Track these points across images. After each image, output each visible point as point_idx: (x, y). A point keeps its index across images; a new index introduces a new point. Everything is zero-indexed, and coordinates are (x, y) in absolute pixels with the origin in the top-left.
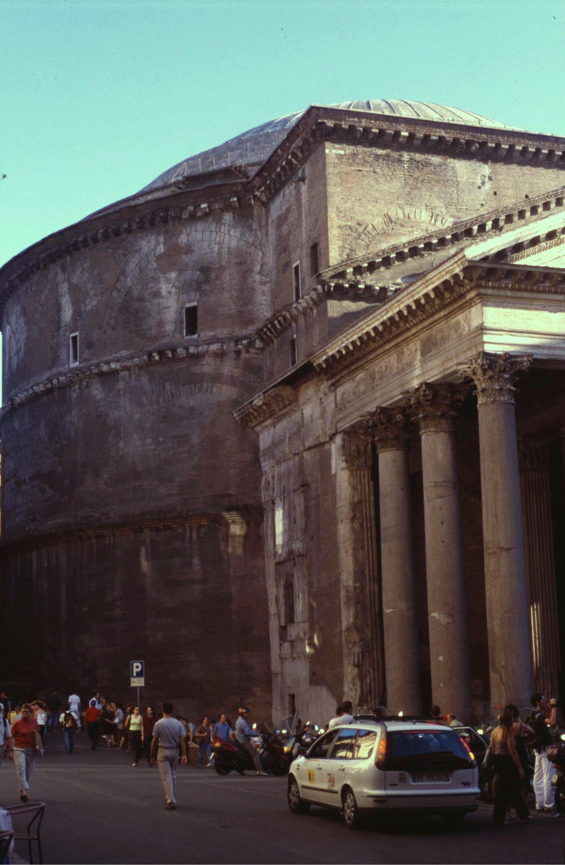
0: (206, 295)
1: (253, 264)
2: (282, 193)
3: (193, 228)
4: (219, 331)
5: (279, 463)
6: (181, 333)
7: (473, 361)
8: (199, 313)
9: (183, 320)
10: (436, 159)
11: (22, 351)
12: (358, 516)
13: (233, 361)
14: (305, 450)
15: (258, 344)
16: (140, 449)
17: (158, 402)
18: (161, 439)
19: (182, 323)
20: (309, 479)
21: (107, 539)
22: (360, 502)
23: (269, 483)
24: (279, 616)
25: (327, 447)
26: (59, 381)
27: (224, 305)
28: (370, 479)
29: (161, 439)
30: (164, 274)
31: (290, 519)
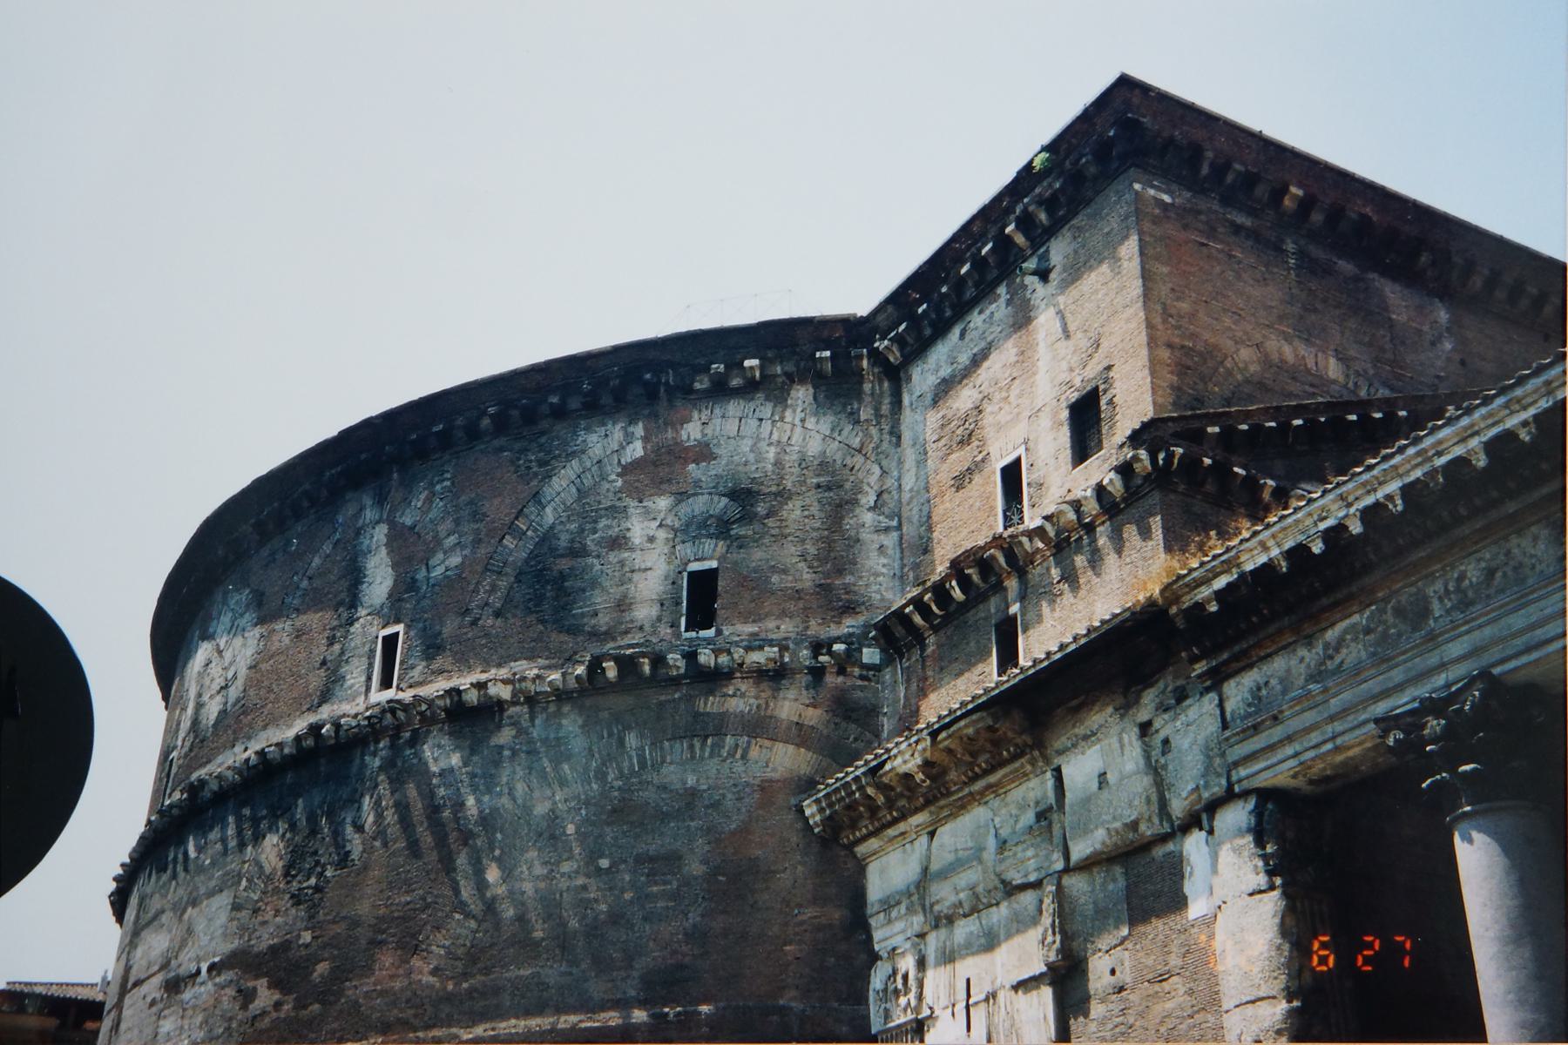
0: (740, 547)
1: (858, 489)
2: (957, 331)
3: (717, 411)
4: (771, 624)
6: (674, 625)
8: (721, 583)
9: (681, 598)
10: (1346, 267)
11: (240, 683)
13: (804, 692)
14: (1067, 870)
15: (870, 655)
18: (604, 863)
19: (678, 604)
27: (785, 571)
29: (604, 863)
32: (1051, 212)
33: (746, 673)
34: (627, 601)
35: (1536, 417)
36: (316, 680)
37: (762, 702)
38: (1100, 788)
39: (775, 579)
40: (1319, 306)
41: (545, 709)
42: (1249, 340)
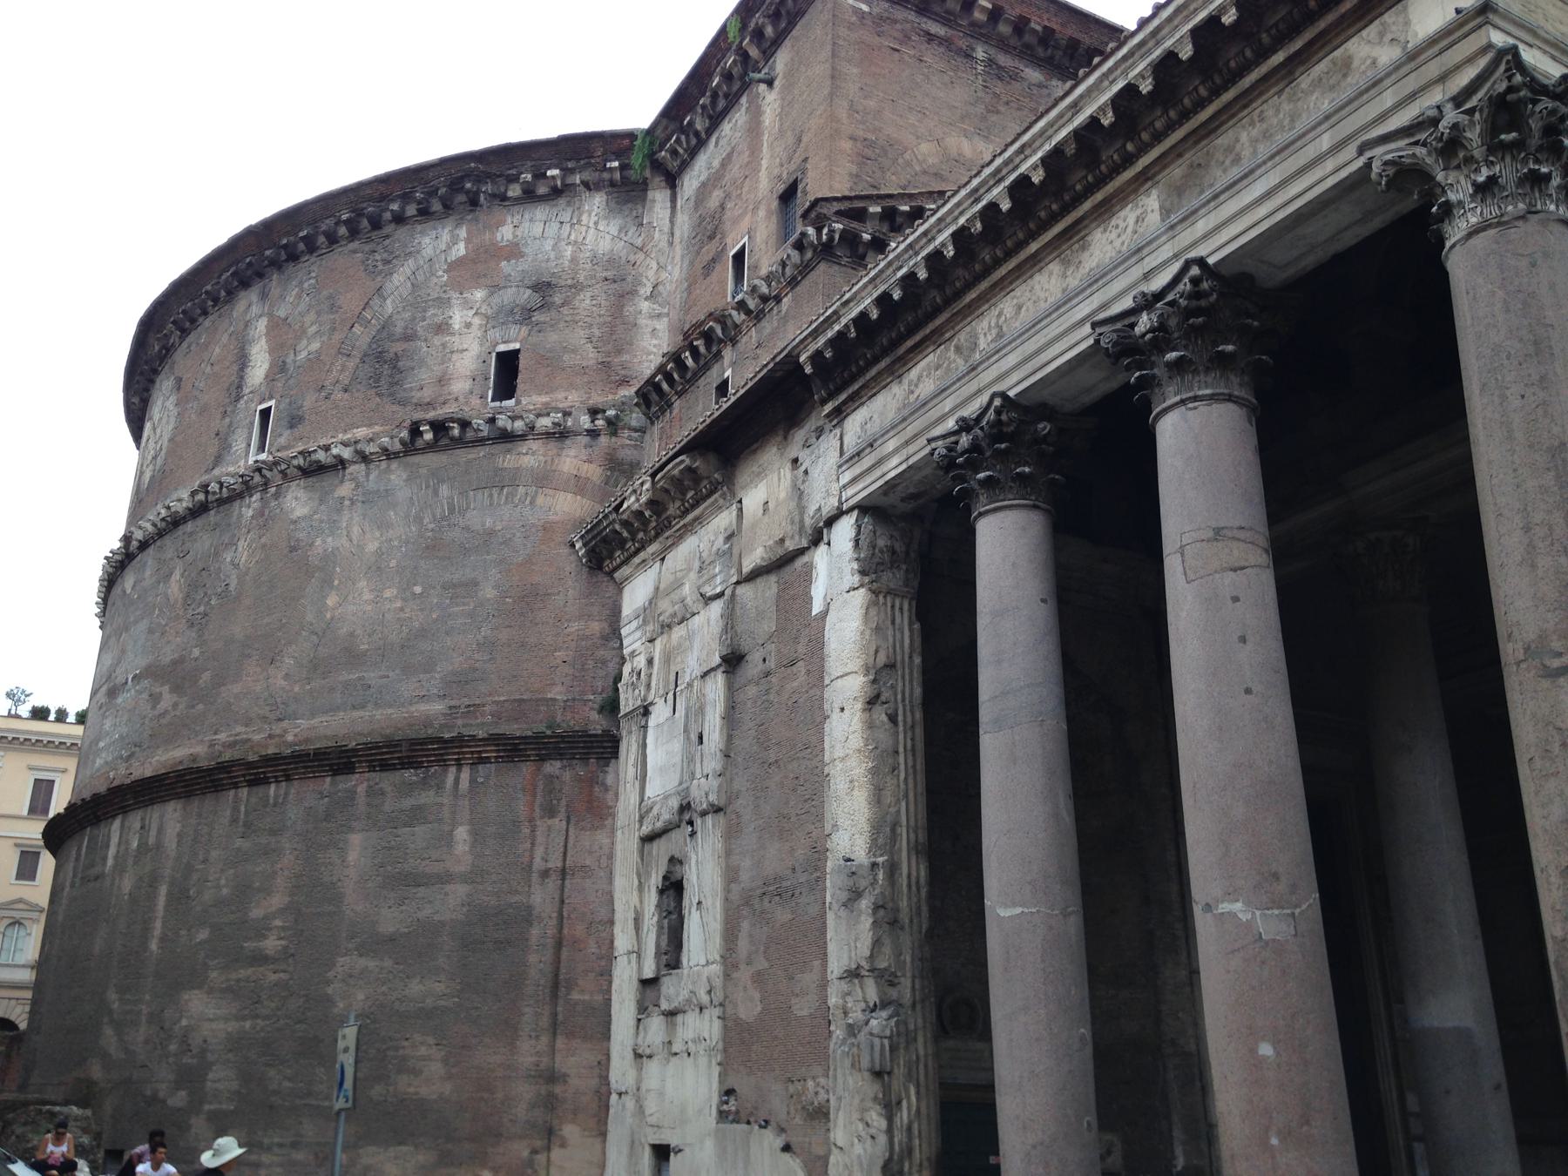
1: (638, 282)
2: (713, 140)
3: (527, 216)
4: (560, 395)
5: (666, 627)
7: (1449, 106)
8: (523, 362)
9: (489, 373)
12: (883, 698)
13: (583, 451)
15: (636, 418)
16: (369, 608)
17: (419, 519)
18: (418, 589)
19: (487, 379)
20: (745, 645)
21: (273, 787)
22: (890, 666)
23: (639, 674)
24: (639, 957)
25: (805, 559)
26: (221, 488)
27: (574, 351)
28: (914, 617)
29: (418, 589)
30: (461, 294)
31: (688, 738)
32: (775, 25)
33: (537, 435)
34: (448, 377)
35: (1043, 160)
36: (213, 450)
37: (549, 459)
38: (764, 514)
39: (566, 357)
40: (1002, 109)
41: (378, 466)
42: (930, 136)
